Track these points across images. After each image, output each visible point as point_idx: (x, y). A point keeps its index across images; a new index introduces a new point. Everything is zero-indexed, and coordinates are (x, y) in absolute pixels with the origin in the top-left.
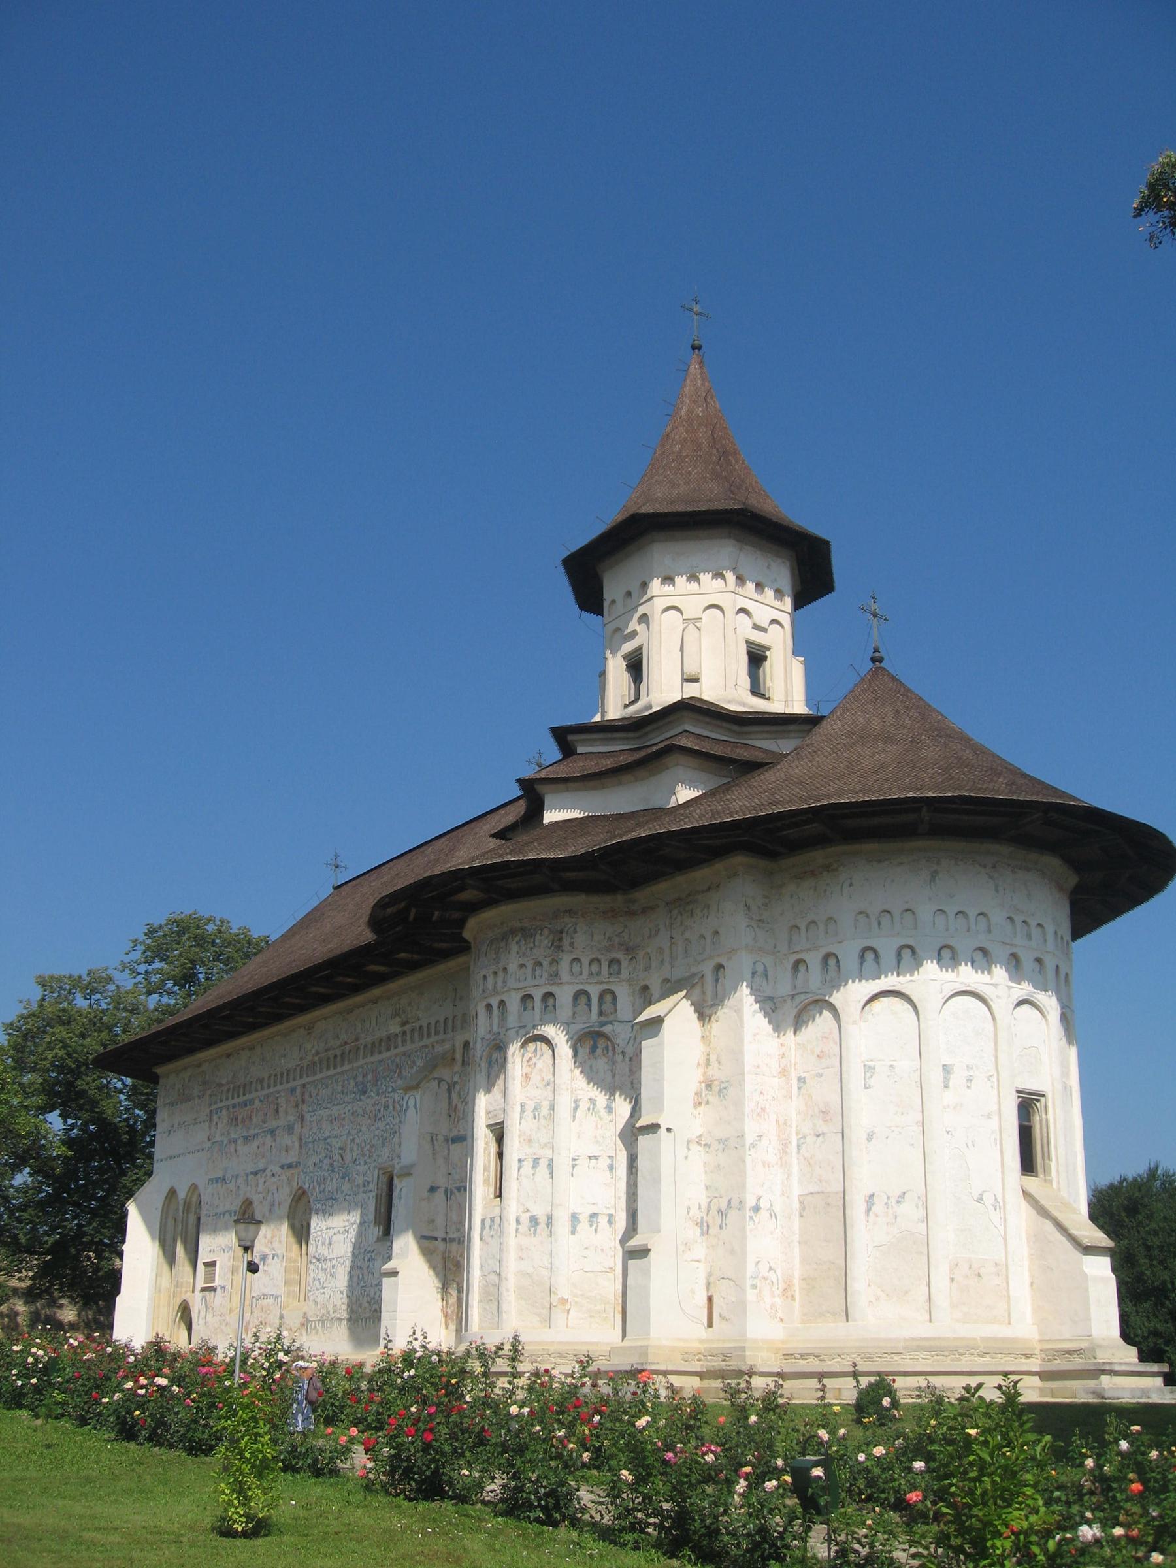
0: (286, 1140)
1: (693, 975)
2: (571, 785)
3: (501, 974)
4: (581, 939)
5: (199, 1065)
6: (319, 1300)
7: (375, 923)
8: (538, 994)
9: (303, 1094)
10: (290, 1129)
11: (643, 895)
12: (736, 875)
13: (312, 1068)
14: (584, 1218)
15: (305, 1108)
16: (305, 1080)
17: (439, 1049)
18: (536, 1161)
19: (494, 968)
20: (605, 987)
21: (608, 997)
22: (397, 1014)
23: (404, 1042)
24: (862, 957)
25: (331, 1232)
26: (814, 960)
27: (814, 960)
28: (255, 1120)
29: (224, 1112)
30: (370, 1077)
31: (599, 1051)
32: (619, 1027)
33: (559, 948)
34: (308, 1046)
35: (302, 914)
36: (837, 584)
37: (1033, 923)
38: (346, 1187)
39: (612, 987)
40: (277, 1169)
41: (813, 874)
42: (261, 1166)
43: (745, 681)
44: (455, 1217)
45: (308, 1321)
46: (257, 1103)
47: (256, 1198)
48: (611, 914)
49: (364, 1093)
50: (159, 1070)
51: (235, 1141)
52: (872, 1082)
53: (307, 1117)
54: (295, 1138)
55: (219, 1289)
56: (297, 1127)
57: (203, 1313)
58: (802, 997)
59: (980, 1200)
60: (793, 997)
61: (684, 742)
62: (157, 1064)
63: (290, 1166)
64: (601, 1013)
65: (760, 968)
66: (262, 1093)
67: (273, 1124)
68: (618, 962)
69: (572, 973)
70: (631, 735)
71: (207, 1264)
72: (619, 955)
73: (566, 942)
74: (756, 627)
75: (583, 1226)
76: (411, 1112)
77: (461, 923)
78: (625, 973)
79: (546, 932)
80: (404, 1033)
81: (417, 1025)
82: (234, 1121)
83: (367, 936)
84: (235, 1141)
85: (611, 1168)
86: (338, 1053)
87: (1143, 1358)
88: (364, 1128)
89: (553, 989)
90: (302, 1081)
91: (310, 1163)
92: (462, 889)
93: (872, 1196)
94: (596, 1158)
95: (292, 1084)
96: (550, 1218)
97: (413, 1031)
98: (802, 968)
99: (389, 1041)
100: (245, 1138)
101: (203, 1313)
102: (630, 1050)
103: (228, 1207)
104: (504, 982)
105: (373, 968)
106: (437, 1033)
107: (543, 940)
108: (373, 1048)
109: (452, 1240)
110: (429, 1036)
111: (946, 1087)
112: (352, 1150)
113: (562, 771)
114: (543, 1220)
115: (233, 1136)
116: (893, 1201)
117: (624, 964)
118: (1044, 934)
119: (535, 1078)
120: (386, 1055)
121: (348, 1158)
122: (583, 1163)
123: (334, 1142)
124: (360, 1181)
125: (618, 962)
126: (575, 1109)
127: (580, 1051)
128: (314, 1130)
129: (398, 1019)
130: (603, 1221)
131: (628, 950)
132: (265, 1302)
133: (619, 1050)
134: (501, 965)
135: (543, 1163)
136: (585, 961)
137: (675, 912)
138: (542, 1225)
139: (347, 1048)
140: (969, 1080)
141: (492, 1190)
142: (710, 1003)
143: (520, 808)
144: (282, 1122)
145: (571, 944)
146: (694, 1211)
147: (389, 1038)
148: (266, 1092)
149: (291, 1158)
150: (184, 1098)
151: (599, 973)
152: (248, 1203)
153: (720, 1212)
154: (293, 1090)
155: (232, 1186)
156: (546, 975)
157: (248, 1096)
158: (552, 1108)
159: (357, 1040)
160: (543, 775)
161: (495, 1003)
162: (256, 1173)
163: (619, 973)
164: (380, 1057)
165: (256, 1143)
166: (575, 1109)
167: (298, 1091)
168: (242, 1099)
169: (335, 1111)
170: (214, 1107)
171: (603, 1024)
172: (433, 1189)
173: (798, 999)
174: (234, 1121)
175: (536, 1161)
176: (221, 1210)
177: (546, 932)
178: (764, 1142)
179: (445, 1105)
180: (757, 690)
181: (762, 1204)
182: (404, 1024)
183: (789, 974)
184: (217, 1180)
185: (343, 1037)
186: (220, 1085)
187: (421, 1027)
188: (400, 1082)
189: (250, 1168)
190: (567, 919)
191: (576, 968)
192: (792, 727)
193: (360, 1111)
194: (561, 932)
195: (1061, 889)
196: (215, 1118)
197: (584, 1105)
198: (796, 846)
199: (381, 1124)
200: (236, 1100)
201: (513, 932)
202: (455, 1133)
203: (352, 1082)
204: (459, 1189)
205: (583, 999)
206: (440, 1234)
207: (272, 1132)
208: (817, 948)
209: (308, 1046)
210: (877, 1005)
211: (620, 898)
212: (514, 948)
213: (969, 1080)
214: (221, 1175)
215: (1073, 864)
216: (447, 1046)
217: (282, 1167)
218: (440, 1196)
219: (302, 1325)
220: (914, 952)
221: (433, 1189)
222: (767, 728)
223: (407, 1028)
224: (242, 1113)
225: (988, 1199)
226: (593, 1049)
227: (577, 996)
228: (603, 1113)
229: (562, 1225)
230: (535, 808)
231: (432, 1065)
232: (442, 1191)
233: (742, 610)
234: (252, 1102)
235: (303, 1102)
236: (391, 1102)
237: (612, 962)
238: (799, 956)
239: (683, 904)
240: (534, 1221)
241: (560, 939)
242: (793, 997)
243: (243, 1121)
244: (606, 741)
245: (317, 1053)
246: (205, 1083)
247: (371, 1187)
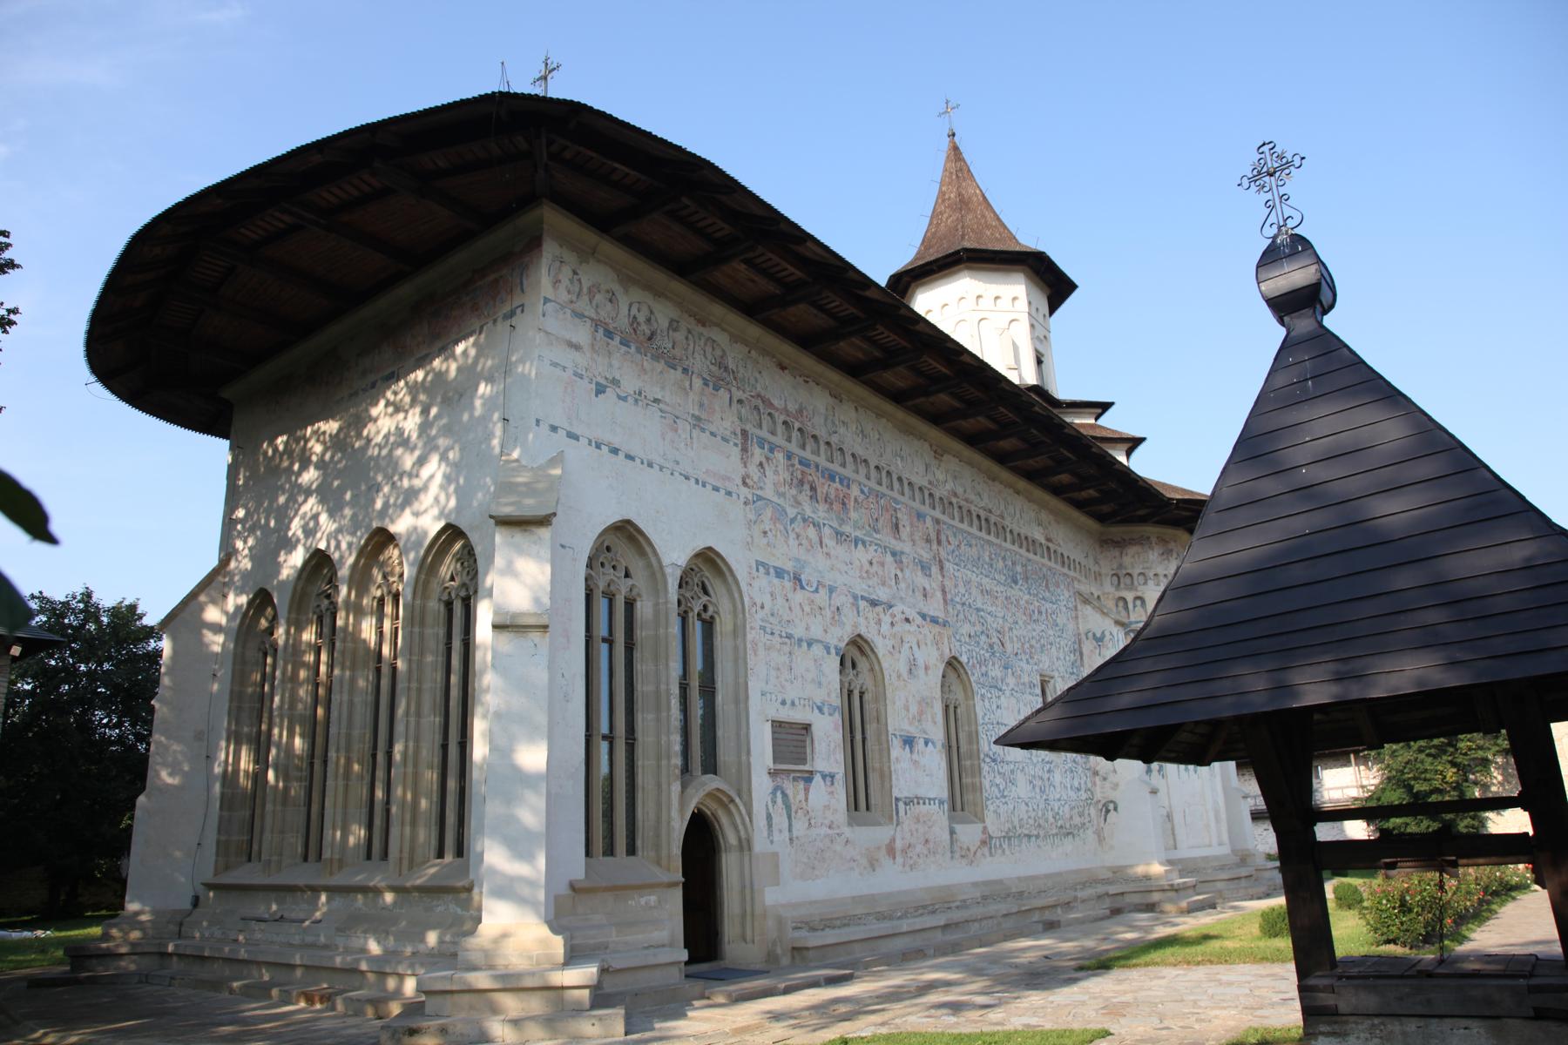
6: (1001, 811)
28: (853, 515)
42: (882, 594)
45: (991, 838)
46: (855, 491)
55: (818, 778)
57: (780, 819)
103: (816, 632)
132: (923, 808)
152: (859, 644)
185: (986, 502)
189: (860, 588)
217: (924, 616)
219: (984, 843)
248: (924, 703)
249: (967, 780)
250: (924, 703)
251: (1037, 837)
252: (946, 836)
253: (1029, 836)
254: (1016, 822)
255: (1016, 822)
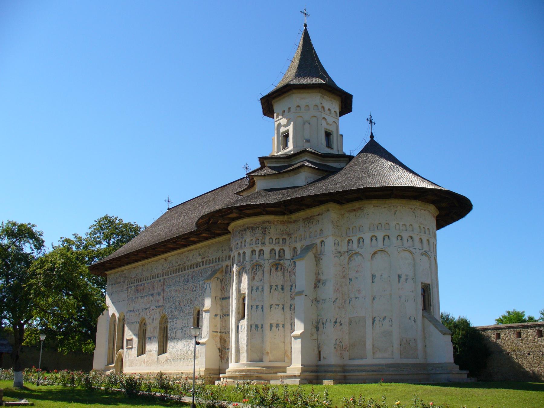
0: (158, 298)
1: (313, 244)
2: (266, 177)
3: (243, 243)
4: (272, 231)
5: (123, 271)
7: (197, 224)
8: (257, 250)
9: (164, 282)
10: (159, 294)
11: (294, 217)
12: (328, 210)
13: (167, 273)
14: (274, 325)
15: (165, 287)
16: (164, 277)
17: (216, 267)
18: (257, 306)
19: (241, 240)
20: (281, 247)
21: (282, 251)
22: (200, 255)
23: (203, 265)
24: (372, 239)
25: (176, 329)
26: (355, 239)
27: (355, 239)
29: (133, 287)
30: (190, 276)
31: (279, 269)
32: (286, 261)
33: (265, 234)
34: (165, 265)
35: (156, 218)
36: (353, 110)
37: (426, 228)
38: (181, 314)
39: (283, 248)
40: (154, 307)
41: (355, 210)
42: (148, 306)
43: (324, 143)
44: (224, 325)
46: (146, 285)
47: (146, 317)
48: (283, 223)
49: (188, 282)
50: (107, 273)
51: (138, 298)
52: (375, 280)
53: (166, 290)
54: (161, 297)
56: (162, 293)
57: (127, 356)
58: (351, 252)
59: (410, 319)
60: (348, 252)
61: (307, 164)
62: (107, 270)
63: (159, 307)
64: (279, 256)
65: (336, 242)
66: (147, 282)
67: (152, 292)
68: (285, 239)
69: (269, 243)
70: (287, 160)
71: (128, 340)
72: (286, 237)
73: (267, 232)
74: (327, 124)
75: (274, 328)
76: (208, 289)
77: (228, 224)
78: (288, 242)
79: (260, 228)
80: (203, 262)
81: (208, 259)
82: (137, 291)
83: (196, 228)
84: (138, 298)
85: (283, 308)
86: (177, 267)
87: (461, 369)
88: (188, 294)
89: (263, 248)
90: (164, 277)
91: (167, 306)
92: (232, 213)
93: (375, 318)
94: (278, 305)
95: (159, 278)
96: (262, 325)
97: (206, 261)
98: (351, 242)
99: (197, 265)
100: (141, 297)
101: (127, 356)
102: (290, 269)
103: (136, 320)
104: (245, 245)
105: (192, 239)
106: (216, 262)
107: (259, 231)
108: (191, 267)
109: (222, 333)
110: (212, 263)
111: (399, 282)
112: (183, 301)
113: (263, 172)
114: (260, 326)
115: (137, 296)
116: (382, 319)
117: (287, 239)
118: (429, 232)
119: (256, 278)
120: (196, 269)
121: (182, 304)
122: (274, 307)
123: (176, 299)
124: (187, 312)
125: (285, 239)
126: (271, 289)
127: (272, 269)
128: (169, 294)
129: (200, 257)
130: (281, 326)
131: (289, 235)
133: (286, 269)
134: (244, 240)
135: (260, 307)
136: (274, 239)
137: (306, 222)
138: (260, 329)
139: (181, 266)
140: (406, 280)
141: (241, 315)
142: (319, 253)
143: (246, 185)
144: (156, 291)
145: (269, 233)
146: (314, 323)
147: (197, 264)
148: (149, 281)
149: (160, 304)
150: (117, 283)
151: (279, 243)
153: (323, 323)
154: (160, 281)
155: (137, 313)
156: (260, 243)
157: (142, 283)
158: (263, 288)
159: (185, 263)
160: (256, 174)
161: (241, 252)
162: (146, 309)
163: (285, 243)
164: (194, 270)
165: (146, 299)
166: (271, 289)
167: (162, 280)
168: (140, 283)
169: (176, 288)
170: (129, 286)
171: (280, 260)
172: (216, 315)
173: (349, 253)
174: (137, 291)
175: (257, 306)
176: (133, 321)
177: (260, 228)
178: (338, 300)
179: (220, 287)
180: (329, 145)
181: (338, 320)
182: (203, 259)
183: (346, 243)
184: (131, 311)
185: (179, 262)
186: (131, 278)
187: (210, 260)
188: (201, 278)
189: (144, 307)
190: (267, 224)
191: (271, 241)
192: (342, 159)
193: (186, 288)
194: (266, 228)
195: (434, 217)
196: (129, 290)
197: (274, 287)
198: (349, 201)
199: (194, 293)
200: (138, 284)
201: (248, 228)
202: (223, 296)
203: (183, 278)
204: (225, 315)
205: (273, 252)
206: (219, 330)
207: (152, 295)
208: (356, 236)
209: (165, 265)
210: (376, 256)
211: (286, 217)
212: (249, 233)
213: (406, 280)
214: (132, 309)
215: (439, 208)
216: (220, 266)
217: (156, 307)
218: (218, 317)
220: (389, 238)
221: (216, 315)
222: (333, 159)
223: (204, 260)
224: (140, 288)
225: (412, 318)
226: (277, 269)
227: (271, 251)
228: (280, 290)
229: (267, 327)
230: (252, 184)
231: (214, 273)
232: (219, 316)
233: (324, 118)
234: (144, 284)
235: (164, 285)
236: (198, 285)
237: (283, 239)
238: (350, 238)
239: (309, 220)
240: (257, 326)
241: (265, 231)
242: (348, 252)
243: (141, 291)
244: (277, 162)
245: (169, 268)
246: (125, 277)
247: (191, 314)
248: (155, 328)
249: (162, 344)
250: (155, 328)
251: (184, 359)
252: (156, 359)
253: (181, 359)
254: (176, 355)
255: (176, 355)
